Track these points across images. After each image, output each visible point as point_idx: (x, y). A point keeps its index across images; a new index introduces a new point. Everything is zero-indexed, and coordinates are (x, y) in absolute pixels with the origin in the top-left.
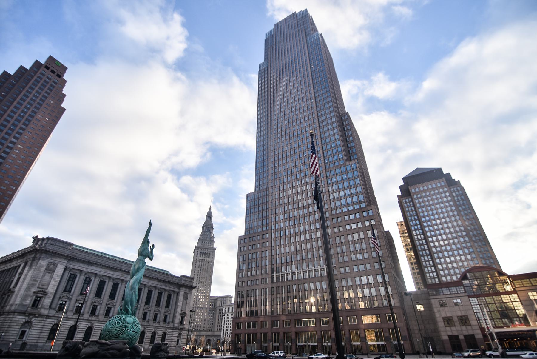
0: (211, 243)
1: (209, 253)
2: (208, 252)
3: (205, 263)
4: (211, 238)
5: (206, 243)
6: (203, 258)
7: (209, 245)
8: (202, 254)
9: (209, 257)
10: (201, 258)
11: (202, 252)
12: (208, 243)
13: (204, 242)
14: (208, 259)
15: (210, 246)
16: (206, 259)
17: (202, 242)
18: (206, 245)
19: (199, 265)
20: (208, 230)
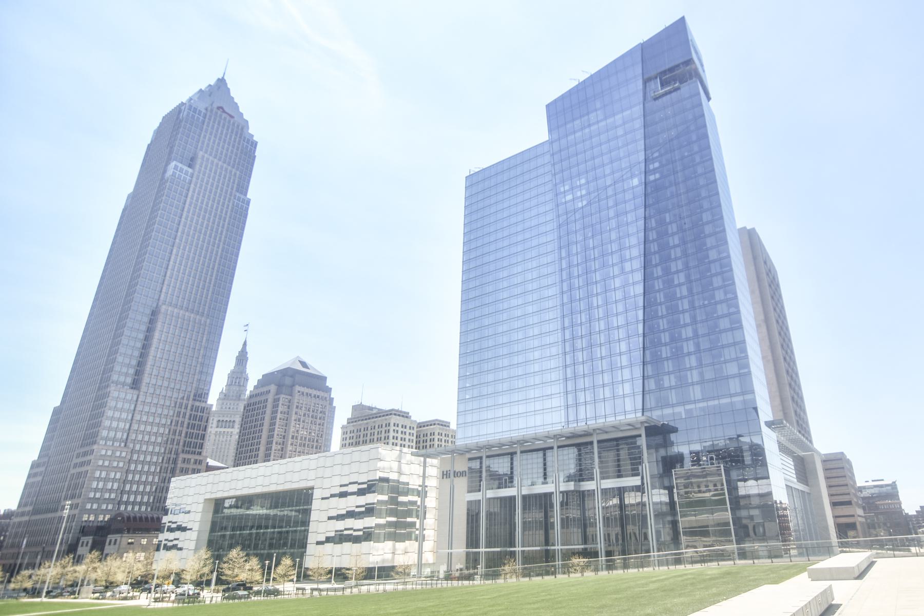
0: (238, 404)
1: (234, 421)
2: (232, 420)
3: (225, 437)
4: (240, 396)
5: (230, 404)
6: (222, 430)
7: (235, 407)
8: (220, 424)
9: (233, 427)
10: (219, 430)
11: (221, 419)
12: (234, 405)
13: (227, 404)
14: (230, 430)
15: (237, 409)
16: (226, 430)
17: (223, 404)
18: (229, 408)
19: (215, 440)
20: (235, 382)
